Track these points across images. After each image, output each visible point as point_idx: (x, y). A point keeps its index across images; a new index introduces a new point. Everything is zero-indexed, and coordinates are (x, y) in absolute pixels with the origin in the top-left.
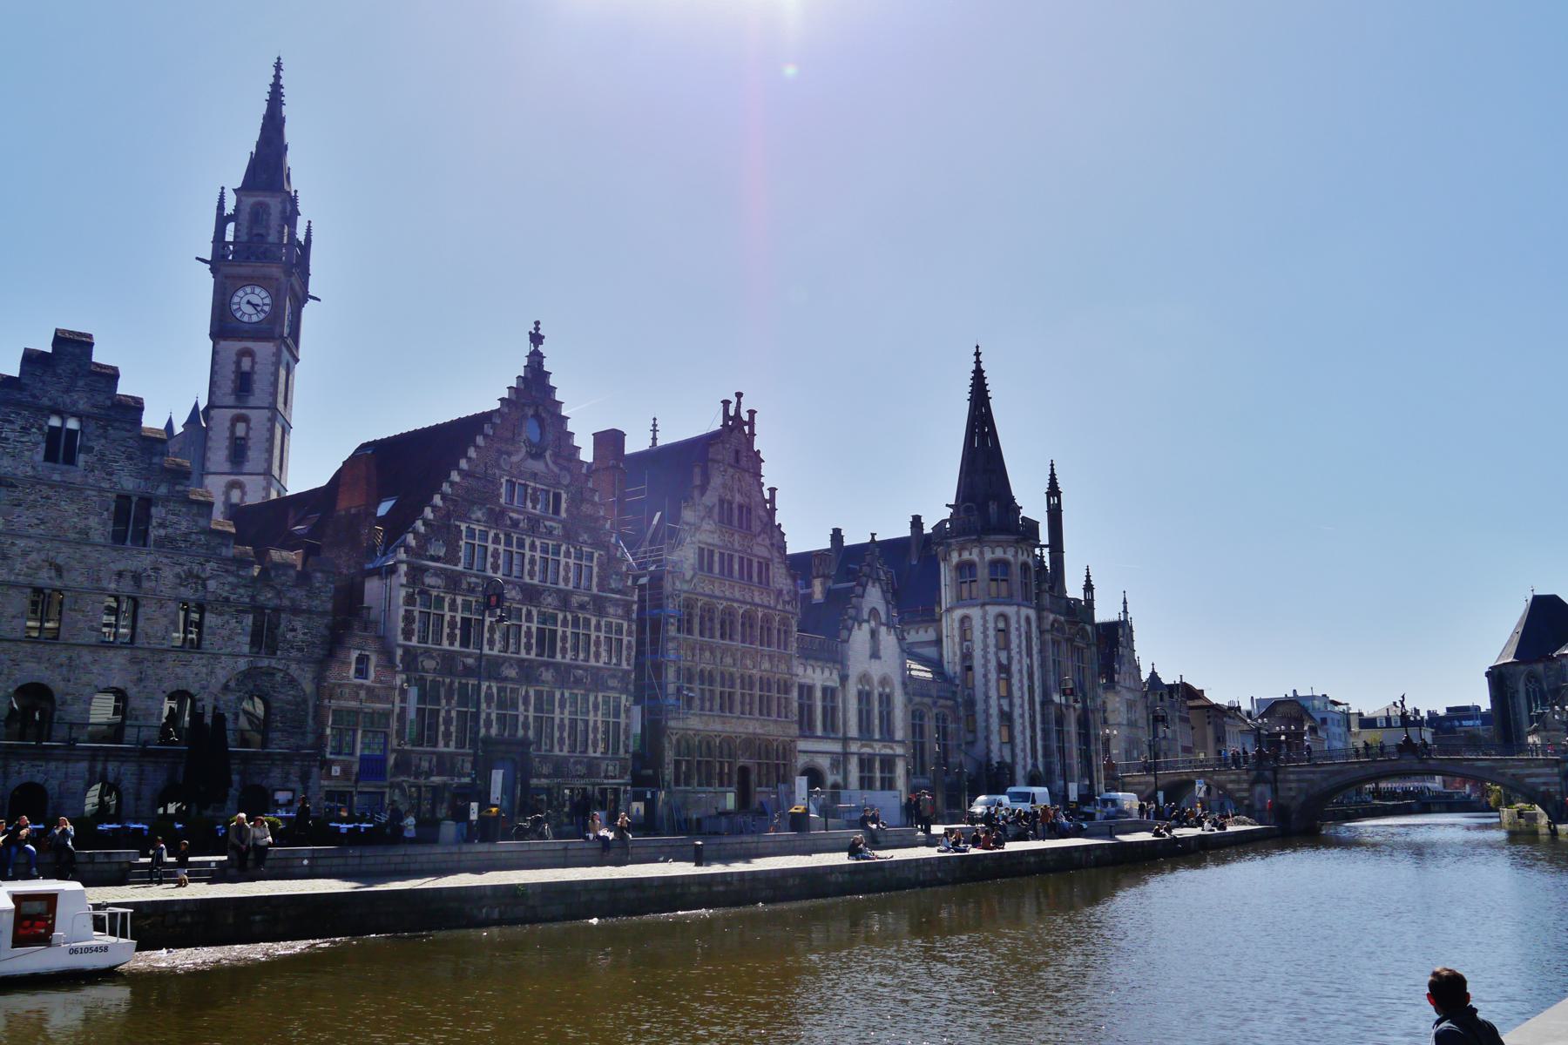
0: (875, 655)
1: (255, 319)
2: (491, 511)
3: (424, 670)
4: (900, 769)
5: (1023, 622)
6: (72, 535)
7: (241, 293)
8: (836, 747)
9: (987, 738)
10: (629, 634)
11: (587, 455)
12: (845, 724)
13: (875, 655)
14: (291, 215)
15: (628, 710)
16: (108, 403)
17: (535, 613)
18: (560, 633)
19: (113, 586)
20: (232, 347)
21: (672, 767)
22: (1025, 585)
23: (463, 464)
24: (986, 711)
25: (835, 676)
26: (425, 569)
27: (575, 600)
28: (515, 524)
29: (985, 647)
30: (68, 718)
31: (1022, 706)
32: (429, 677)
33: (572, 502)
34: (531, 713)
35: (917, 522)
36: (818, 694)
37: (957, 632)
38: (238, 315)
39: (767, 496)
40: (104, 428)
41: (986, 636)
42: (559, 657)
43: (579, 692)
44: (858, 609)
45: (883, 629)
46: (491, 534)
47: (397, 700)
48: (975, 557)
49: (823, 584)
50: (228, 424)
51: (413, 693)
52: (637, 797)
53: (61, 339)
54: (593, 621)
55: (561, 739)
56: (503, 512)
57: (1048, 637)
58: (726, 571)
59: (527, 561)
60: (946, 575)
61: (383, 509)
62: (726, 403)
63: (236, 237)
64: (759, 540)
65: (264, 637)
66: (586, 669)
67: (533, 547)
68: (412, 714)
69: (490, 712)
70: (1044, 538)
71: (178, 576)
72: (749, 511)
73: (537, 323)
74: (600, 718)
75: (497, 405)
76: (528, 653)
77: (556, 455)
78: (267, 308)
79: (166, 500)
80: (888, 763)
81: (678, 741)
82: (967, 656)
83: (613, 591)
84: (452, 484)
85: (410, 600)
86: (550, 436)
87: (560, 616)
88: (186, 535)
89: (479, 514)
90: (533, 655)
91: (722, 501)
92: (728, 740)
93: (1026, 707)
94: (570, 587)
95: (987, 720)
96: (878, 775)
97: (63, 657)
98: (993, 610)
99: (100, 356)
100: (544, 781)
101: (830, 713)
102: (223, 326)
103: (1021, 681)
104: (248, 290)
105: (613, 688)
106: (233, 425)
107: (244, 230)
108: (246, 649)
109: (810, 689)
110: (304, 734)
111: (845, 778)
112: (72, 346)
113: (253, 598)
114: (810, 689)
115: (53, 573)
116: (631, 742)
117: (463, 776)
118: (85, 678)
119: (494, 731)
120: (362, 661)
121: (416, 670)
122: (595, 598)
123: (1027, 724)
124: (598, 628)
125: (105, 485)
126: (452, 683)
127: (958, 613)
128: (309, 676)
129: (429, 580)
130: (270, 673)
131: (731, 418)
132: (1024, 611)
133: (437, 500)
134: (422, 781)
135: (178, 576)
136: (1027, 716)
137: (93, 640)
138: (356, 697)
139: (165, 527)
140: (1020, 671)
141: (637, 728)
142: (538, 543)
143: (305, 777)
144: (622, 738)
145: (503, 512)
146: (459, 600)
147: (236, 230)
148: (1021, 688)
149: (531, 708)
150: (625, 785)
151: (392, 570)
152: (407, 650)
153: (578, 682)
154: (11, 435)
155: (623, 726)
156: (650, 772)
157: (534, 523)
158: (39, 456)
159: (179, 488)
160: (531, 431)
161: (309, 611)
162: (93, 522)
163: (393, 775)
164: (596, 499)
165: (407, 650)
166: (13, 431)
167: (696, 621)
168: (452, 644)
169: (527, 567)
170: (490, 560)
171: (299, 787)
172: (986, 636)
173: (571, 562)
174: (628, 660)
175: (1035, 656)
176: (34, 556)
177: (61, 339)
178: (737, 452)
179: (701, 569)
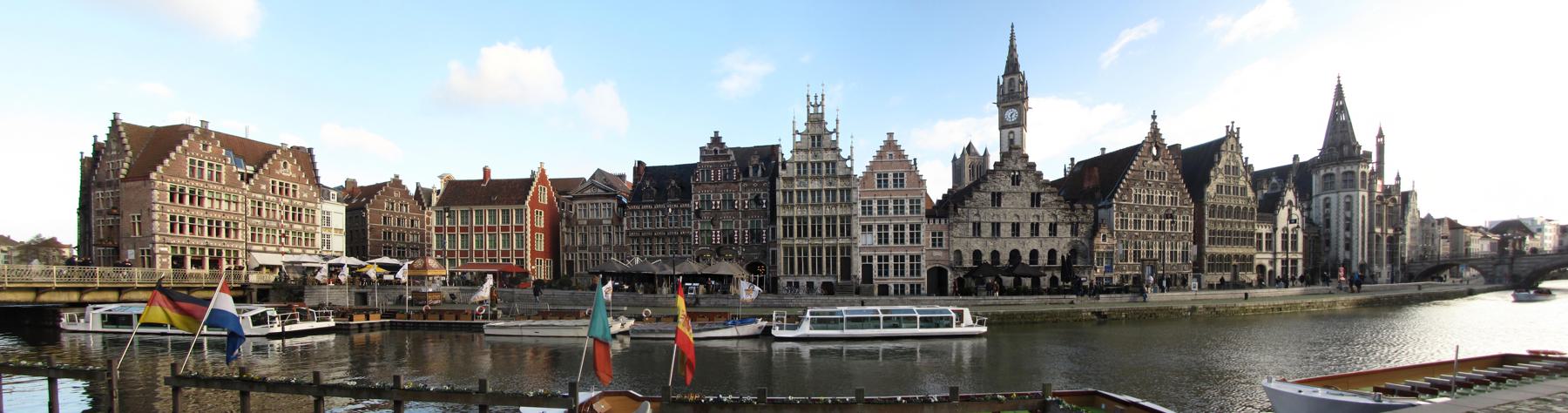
20: (1006, 131)
58: (1228, 192)
60: (1316, 180)
65: (1074, 232)
69: (1143, 250)
82: (1327, 215)
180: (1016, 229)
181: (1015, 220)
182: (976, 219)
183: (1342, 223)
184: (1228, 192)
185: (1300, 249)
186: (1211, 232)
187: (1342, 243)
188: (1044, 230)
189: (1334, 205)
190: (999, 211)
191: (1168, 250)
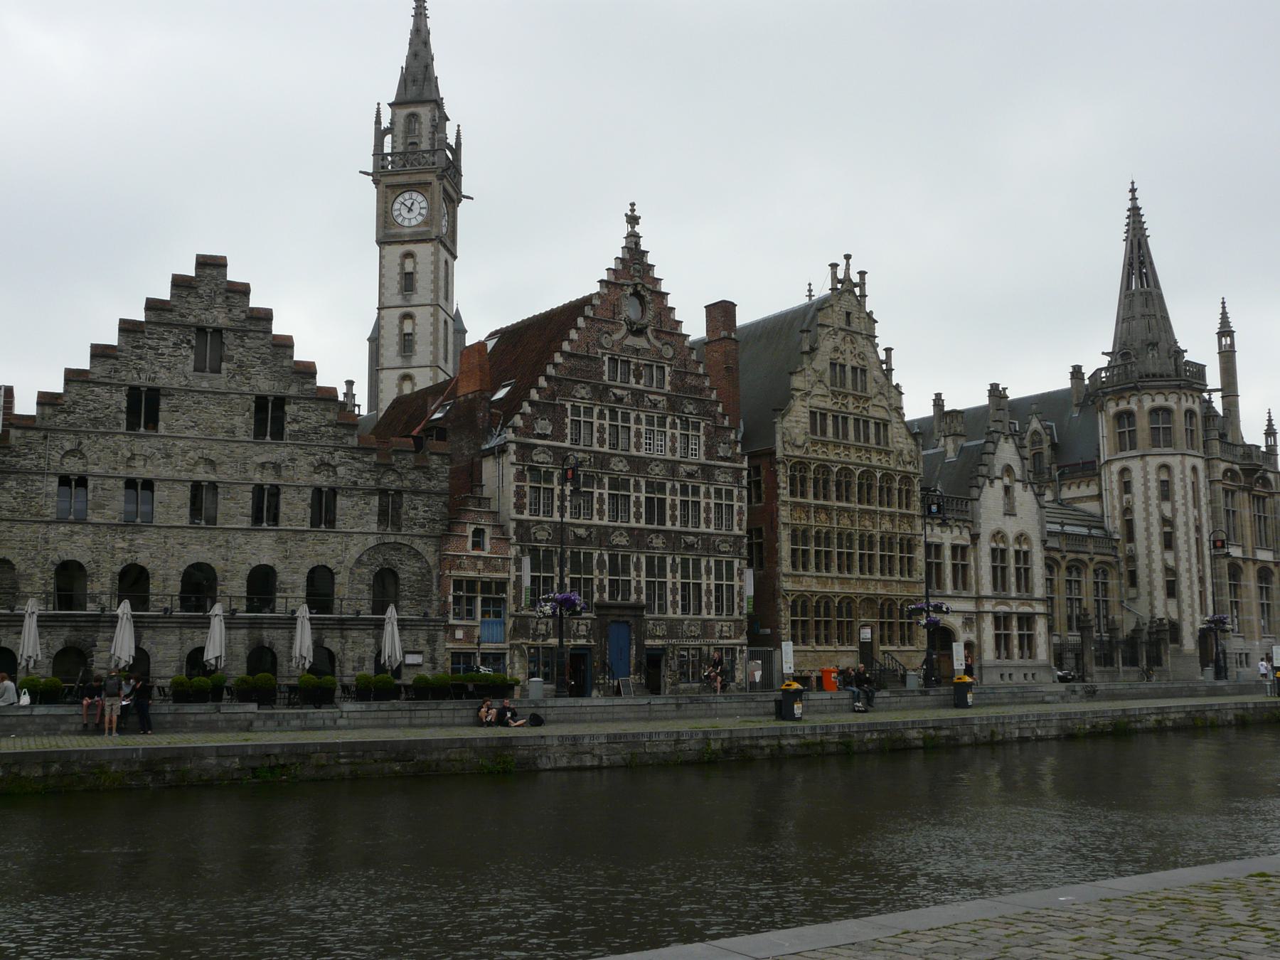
0: (1010, 512)
1: (414, 222)
2: (595, 388)
3: (536, 540)
4: (1041, 626)
5: (1188, 472)
7: (400, 199)
8: (970, 606)
9: (1150, 594)
10: (740, 499)
11: (695, 327)
12: (977, 583)
13: (1010, 512)
14: (441, 119)
15: (741, 574)
16: (243, 316)
17: (643, 483)
18: (668, 502)
19: (258, 476)
20: (396, 251)
21: (789, 626)
22: (1191, 433)
23: (566, 346)
24: (1149, 566)
25: (966, 534)
27: (683, 469)
28: (619, 400)
29: (1147, 498)
30: (229, 592)
31: (1189, 560)
33: (675, 373)
34: (643, 579)
35: (1077, 372)
36: (947, 553)
37: (1115, 485)
38: (399, 220)
39: (882, 356)
40: (241, 338)
41: (1147, 488)
42: (669, 525)
43: (691, 557)
44: (990, 466)
45: (1018, 487)
46: (596, 410)
47: (513, 569)
48: (1134, 406)
49: (955, 442)
50: (397, 322)
51: (526, 561)
52: (753, 656)
53: (204, 262)
54: (703, 489)
55: (674, 603)
56: (607, 387)
57: (1219, 487)
59: (632, 434)
60: (1105, 427)
61: (501, 394)
62: (834, 266)
63: (393, 148)
64: (875, 401)
65: (389, 515)
66: (695, 535)
68: (527, 582)
69: (601, 577)
70: (1213, 378)
71: (311, 464)
72: (864, 371)
73: (633, 205)
74: (713, 582)
75: (596, 288)
76: (638, 521)
77: (658, 332)
78: (424, 212)
79: (296, 399)
80: (1027, 620)
81: (794, 601)
82: (1127, 510)
84: (556, 365)
85: (520, 476)
86: (650, 314)
87: (669, 485)
88: (316, 430)
89: (583, 392)
91: (833, 365)
92: (827, 599)
93: (1194, 560)
94: (677, 457)
95: (1150, 576)
96: (1015, 632)
97: (221, 539)
98: (1153, 462)
99: (233, 275)
100: (658, 642)
101: (961, 573)
102: (387, 235)
103: (1187, 534)
104: (407, 195)
105: (725, 552)
106: (401, 322)
107: (400, 141)
109: (938, 547)
110: (430, 601)
111: (979, 637)
112: (211, 265)
113: (378, 481)
114: (938, 547)
115: (208, 468)
116: (745, 604)
117: (580, 637)
118: (239, 557)
119: (606, 596)
120: (479, 533)
121: (530, 541)
122: (703, 467)
123: (1196, 579)
125: (246, 389)
127: (1116, 467)
128: (432, 549)
129: (539, 457)
130: (397, 547)
131: (840, 281)
132: (1189, 461)
133: (542, 382)
134: (540, 642)
135: (311, 464)
136: (1195, 570)
137: (245, 526)
138: (475, 568)
139: (298, 422)
140: (1186, 524)
141: (749, 591)
142: (643, 416)
143: (432, 641)
144: (737, 600)
147: (393, 141)
148: (1187, 542)
149: (643, 574)
150: (741, 645)
151: (502, 450)
154: (166, 351)
155: (736, 589)
156: (768, 631)
157: (638, 396)
158: (190, 368)
159: (307, 386)
160: (631, 310)
161: (428, 493)
162: (238, 421)
163: (512, 639)
164: (701, 370)
165: (520, 523)
166: (167, 347)
167: (810, 484)
169: (633, 440)
170: (596, 435)
171: (427, 649)
172: (1147, 488)
173: (677, 432)
174: (740, 525)
175: (1204, 508)
176: (191, 454)
177: (204, 262)
178: (848, 314)
179: (814, 431)
180: (201, 499)
181: (202, 474)
182: (73, 466)
183: (1156, 530)
184: (840, 430)
185: (1039, 592)
186: (798, 536)
187: (1159, 580)
188: (295, 509)
189: (1137, 486)
190: (144, 446)
191: (672, 579)
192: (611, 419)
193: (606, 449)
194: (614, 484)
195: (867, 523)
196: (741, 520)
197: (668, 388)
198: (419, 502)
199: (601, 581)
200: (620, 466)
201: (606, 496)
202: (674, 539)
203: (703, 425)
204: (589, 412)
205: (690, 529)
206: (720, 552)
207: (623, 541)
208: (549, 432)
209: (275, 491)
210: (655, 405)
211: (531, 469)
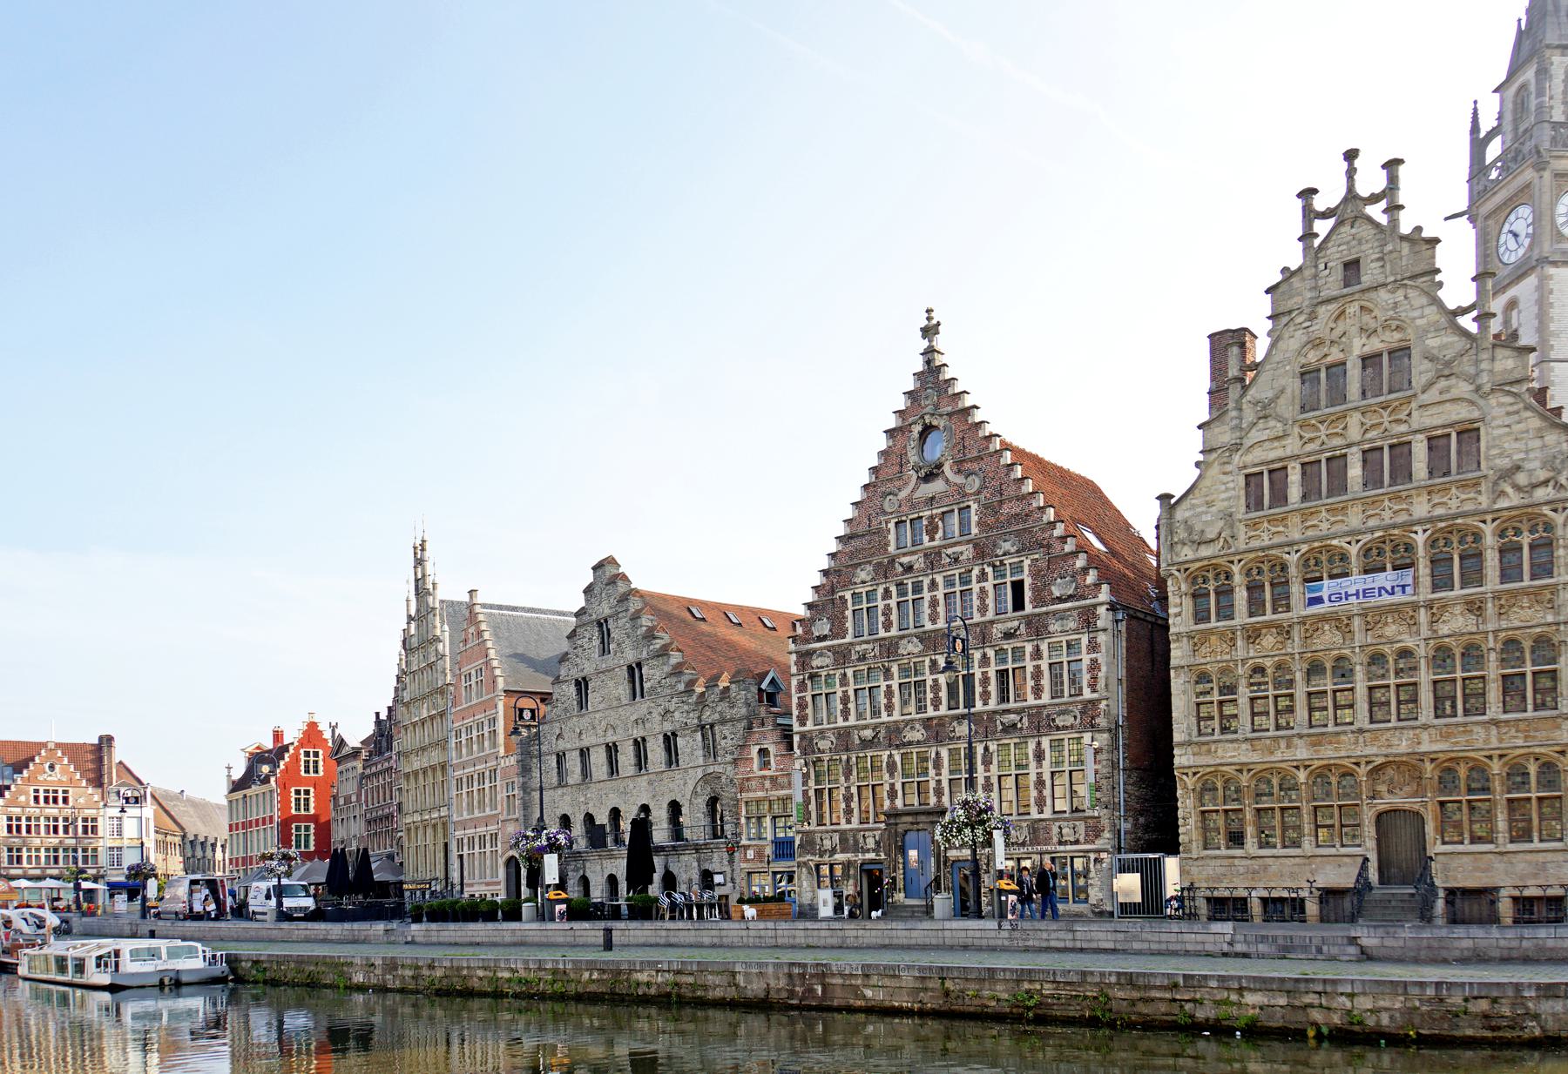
6: (615, 703)
18: (978, 676)
26: (810, 653)
27: (997, 631)
28: (909, 569)
32: (826, 757)
46: (881, 590)
65: (711, 750)
67: (933, 585)
76: (936, 708)
83: (1060, 600)
85: (802, 687)
89: (862, 575)
90: (943, 710)
94: (990, 615)
105: (1065, 728)
108: (701, 761)
120: (763, 752)
124: (1037, 654)
126: (848, 760)
138: (762, 788)
142: (939, 579)
145: (892, 561)
146: (850, 672)
149: (945, 771)
152: (803, 736)
153: (1010, 728)
157: (933, 559)
161: (731, 720)
165: (803, 736)
168: (846, 719)
181: (610, 739)
188: (656, 752)
190: (585, 721)
192: (899, 595)
193: (894, 632)
194: (904, 671)
195: (1390, 630)
196: (1095, 678)
197: (975, 530)
198: (726, 730)
199: (892, 785)
200: (912, 647)
201: (895, 688)
202: (985, 726)
203: (1027, 562)
204: (870, 596)
205: (1012, 705)
206: (1058, 728)
207: (917, 735)
208: (826, 632)
209: (644, 739)
210: (956, 560)
211: (812, 677)
